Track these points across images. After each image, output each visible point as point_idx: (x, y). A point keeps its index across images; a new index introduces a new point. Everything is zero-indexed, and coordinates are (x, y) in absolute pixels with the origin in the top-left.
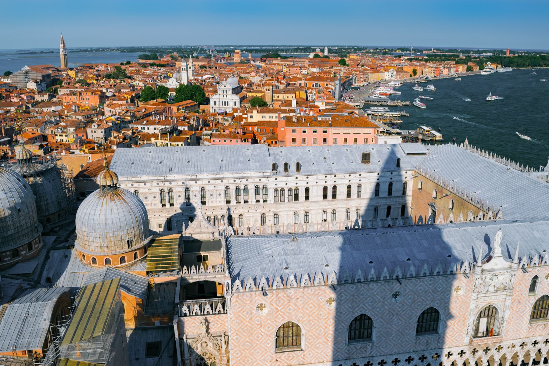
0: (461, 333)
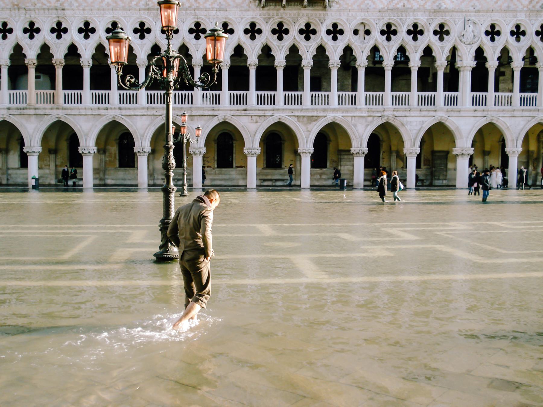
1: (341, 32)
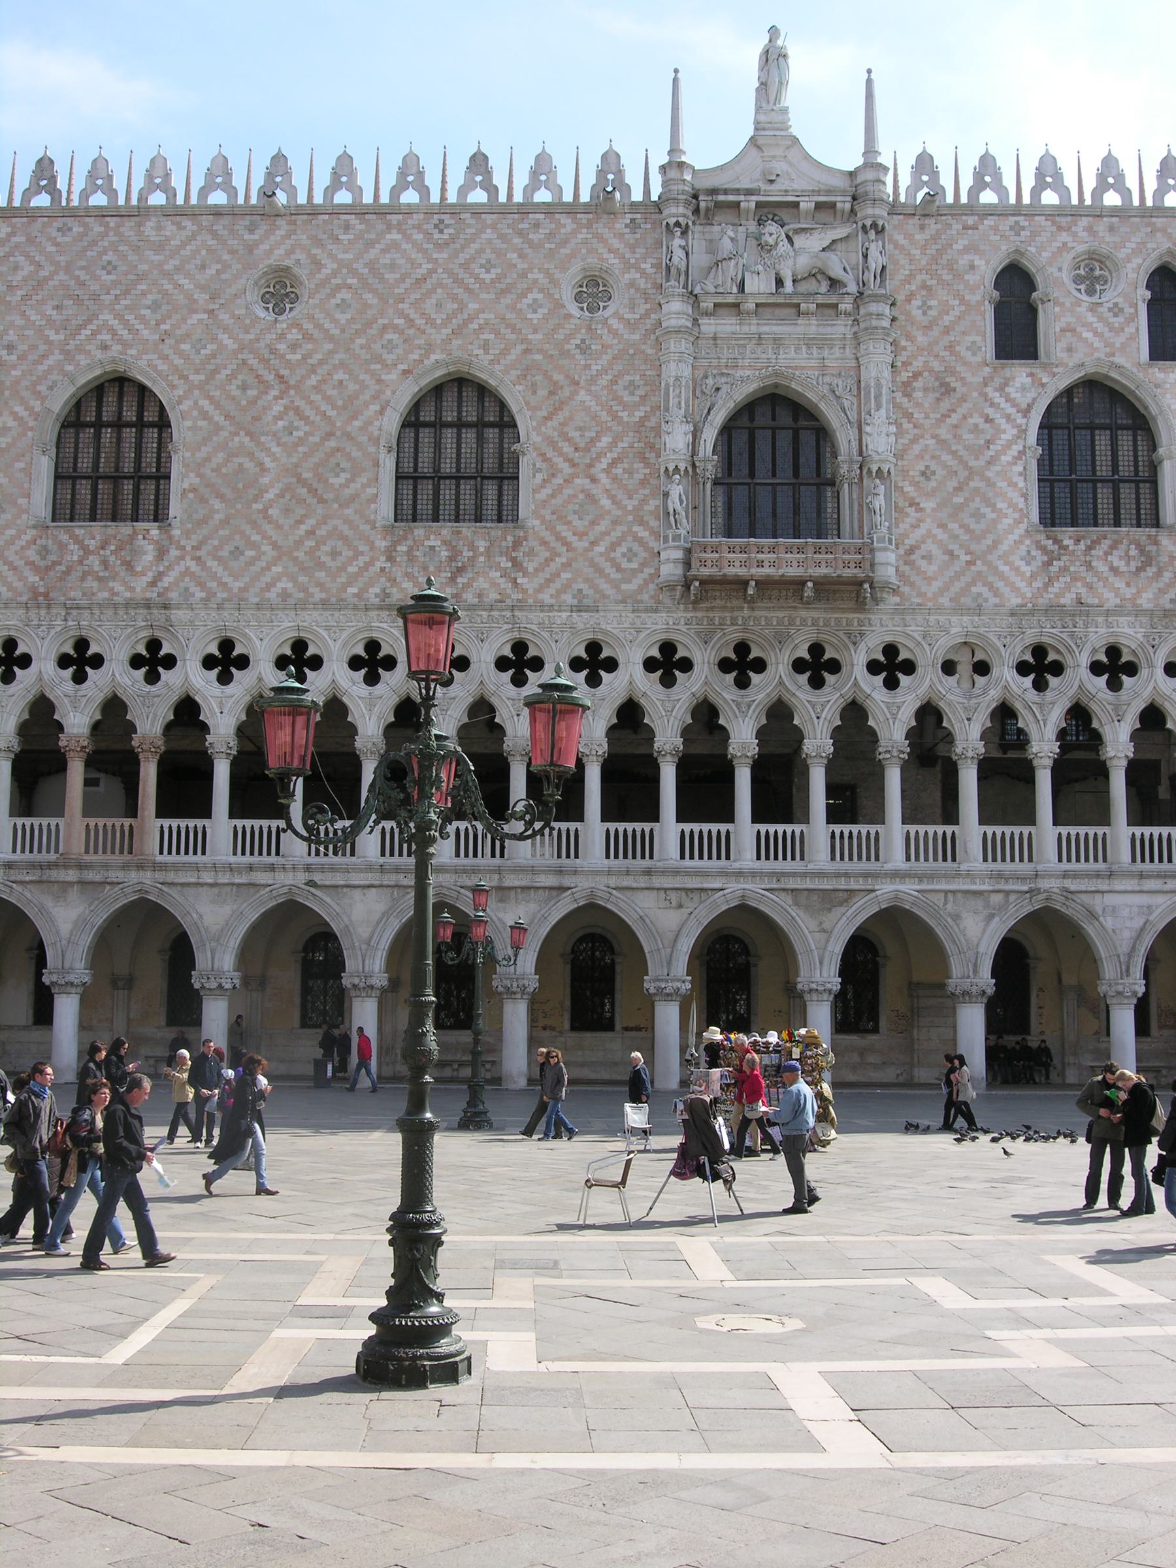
0: (643, 533)
1: (909, 667)
